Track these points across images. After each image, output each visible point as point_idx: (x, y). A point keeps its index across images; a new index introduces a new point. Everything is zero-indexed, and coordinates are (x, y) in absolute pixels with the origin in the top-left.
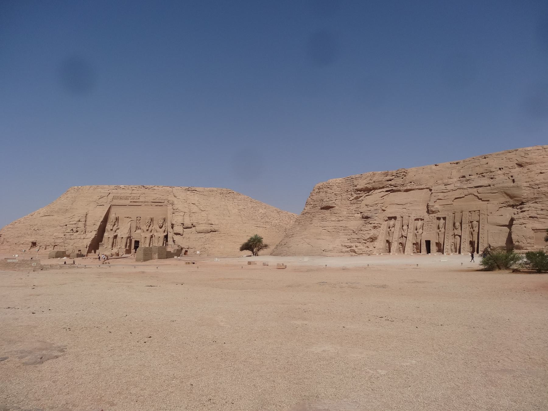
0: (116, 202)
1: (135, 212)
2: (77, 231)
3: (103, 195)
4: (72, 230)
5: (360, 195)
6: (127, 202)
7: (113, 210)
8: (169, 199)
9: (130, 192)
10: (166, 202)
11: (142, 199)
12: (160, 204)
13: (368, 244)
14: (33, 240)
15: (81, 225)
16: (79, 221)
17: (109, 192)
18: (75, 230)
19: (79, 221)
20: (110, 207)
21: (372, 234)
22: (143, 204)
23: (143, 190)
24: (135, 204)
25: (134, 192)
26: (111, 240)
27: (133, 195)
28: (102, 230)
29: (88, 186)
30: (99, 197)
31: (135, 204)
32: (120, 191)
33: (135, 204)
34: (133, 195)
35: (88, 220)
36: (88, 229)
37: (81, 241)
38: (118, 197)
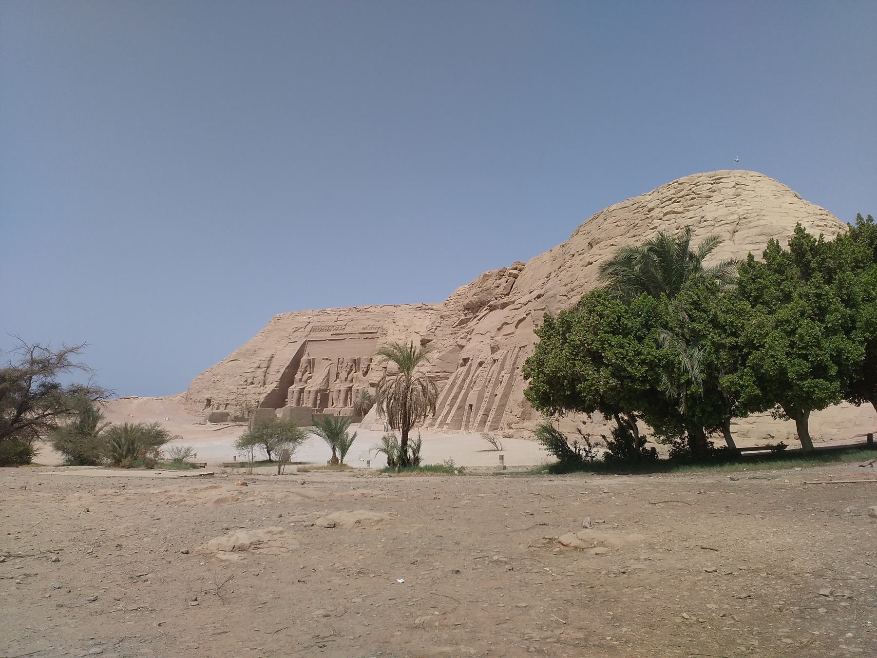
1: (337, 350)
2: (252, 383)
3: (300, 325)
5: (468, 317)
6: (327, 335)
7: (309, 348)
9: (335, 317)
10: (380, 331)
11: (348, 330)
12: (370, 336)
14: (208, 396)
15: (260, 373)
16: (259, 367)
18: (249, 381)
19: (259, 367)
25: (340, 318)
26: (296, 396)
27: (339, 323)
28: (288, 379)
31: (338, 337)
32: (323, 318)
34: (339, 323)
35: (273, 364)
36: (270, 378)
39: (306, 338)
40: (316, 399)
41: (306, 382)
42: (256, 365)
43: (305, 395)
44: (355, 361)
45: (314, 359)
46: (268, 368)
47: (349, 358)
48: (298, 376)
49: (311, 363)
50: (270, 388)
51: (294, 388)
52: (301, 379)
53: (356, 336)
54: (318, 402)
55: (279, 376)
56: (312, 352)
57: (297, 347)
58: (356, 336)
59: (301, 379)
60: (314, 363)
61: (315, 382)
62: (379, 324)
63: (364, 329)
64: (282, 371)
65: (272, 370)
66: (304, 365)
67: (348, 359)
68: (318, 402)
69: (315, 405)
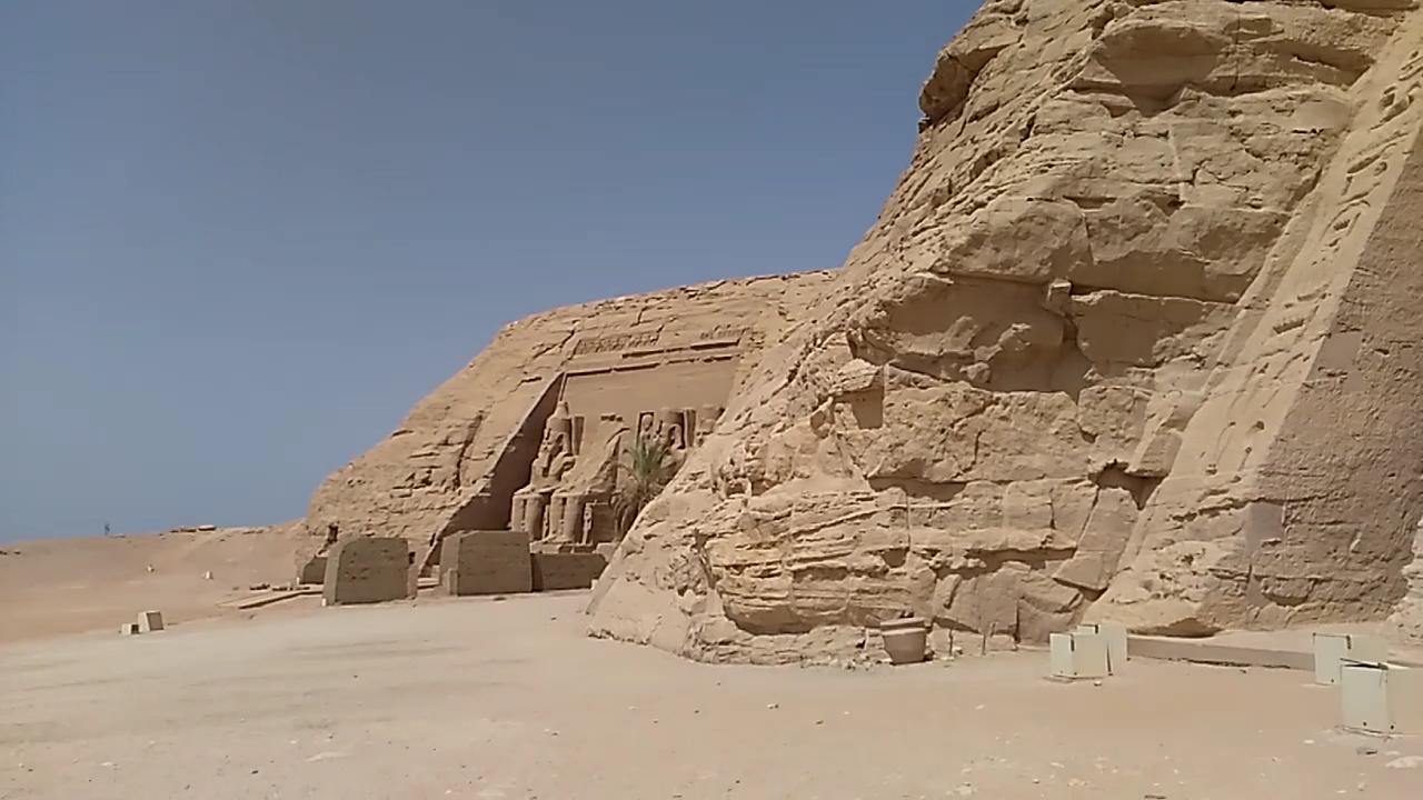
0: (582, 362)
2: (426, 482)
4: (412, 477)
6: (614, 358)
7: (569, 393)
8: (756, 328)
10: (745, 339)
11: (665, 341)
12: (720, 353)
13: (918, 411)
14: (332, 519)
15: (447, 456)
17: (571, 329)
20: (557, 385)
21: (1004, 211)
22: (661, 359)
23: (679, 306)
24: (638, 362)
26: (531, 511)
28: (514, 468)
29: (532, 317)
30: (534, 352)
31: (640, 361)
32: (605, 319)
33: (638, 362)
37: (429, 515)
38: (592, 341)
39: (563, 369)
40: (580, 521)
41: (559, 477)
42: (440, 438)
43: (552, 509)
44: (680, 418)
45: (580, 420)
46: (467, 443)
47: (665, 409)
48: (539, 464)
49: (573, 429)
50: (468, 492)
51: (527, 494)
52: (546, 470)
53: (685, 355)
54: (587, 526)
55: (494, 460)
56: (576, 401)
57: (541, 389)
58: (685, 355)
59: (546, 470)
60: (580, 431)
61: (584, 475)
62: (743, 323)
63: (704, 336)
64: (499, 451)
65: (477, 449)
66: (555, 434)
67: (663, 410)
68: (587, 526)
69: (577, 533)
